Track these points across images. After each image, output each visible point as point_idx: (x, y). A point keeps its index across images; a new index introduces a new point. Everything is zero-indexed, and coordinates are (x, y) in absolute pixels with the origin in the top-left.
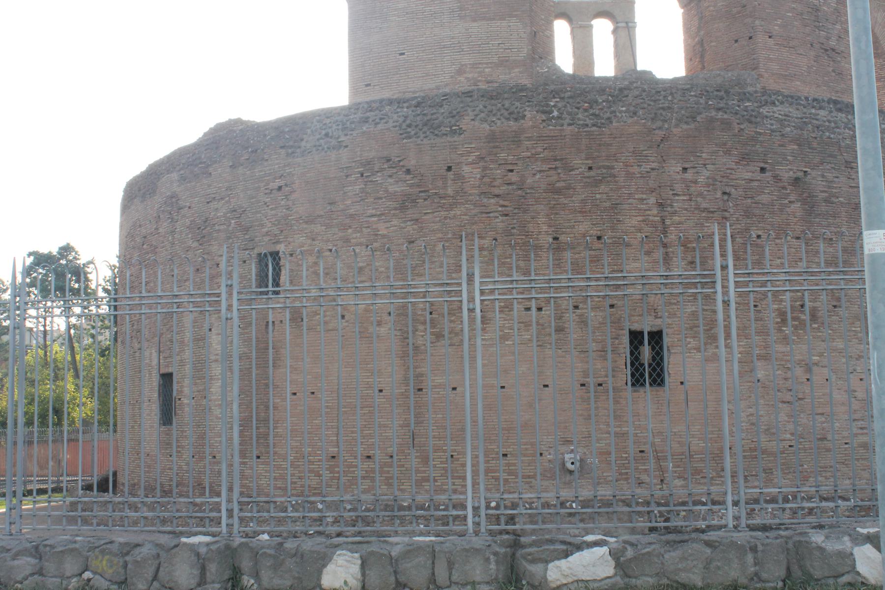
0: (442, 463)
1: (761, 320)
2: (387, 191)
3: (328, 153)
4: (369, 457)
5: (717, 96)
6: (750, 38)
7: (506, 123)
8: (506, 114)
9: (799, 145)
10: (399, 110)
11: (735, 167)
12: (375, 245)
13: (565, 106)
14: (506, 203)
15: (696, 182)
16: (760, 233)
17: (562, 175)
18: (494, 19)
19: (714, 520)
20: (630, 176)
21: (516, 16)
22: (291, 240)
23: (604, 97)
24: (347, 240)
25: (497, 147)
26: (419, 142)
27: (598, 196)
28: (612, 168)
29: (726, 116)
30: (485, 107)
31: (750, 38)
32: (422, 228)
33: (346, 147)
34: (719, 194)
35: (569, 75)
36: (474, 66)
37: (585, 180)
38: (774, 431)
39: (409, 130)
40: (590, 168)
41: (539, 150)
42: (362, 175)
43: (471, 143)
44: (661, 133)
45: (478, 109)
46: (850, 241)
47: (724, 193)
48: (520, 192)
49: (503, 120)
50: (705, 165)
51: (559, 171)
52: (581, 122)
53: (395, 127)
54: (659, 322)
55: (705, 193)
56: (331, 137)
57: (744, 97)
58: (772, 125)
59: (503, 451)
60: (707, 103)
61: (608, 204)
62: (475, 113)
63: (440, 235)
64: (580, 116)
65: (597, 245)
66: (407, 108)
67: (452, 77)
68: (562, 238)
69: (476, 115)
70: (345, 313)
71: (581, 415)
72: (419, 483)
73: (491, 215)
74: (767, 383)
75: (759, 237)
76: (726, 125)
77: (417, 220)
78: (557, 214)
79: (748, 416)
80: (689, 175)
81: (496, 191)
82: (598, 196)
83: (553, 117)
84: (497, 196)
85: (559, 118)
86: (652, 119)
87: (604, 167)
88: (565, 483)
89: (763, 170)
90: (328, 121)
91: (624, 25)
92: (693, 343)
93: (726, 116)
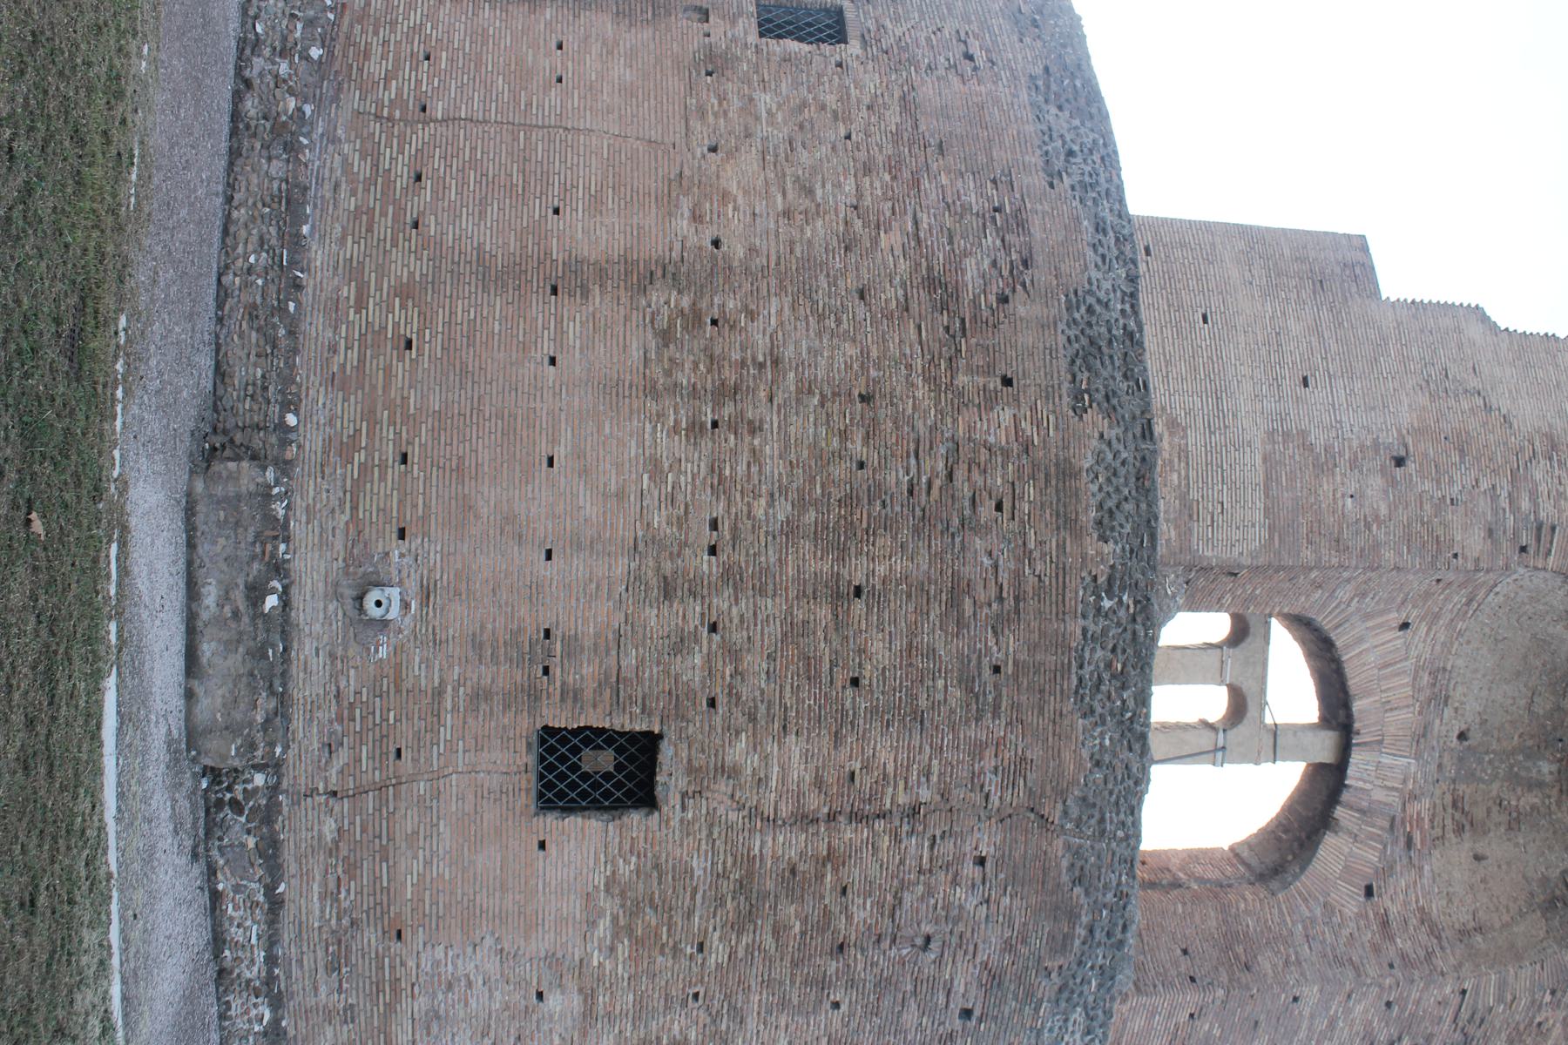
0: (396, 325)
1: (667, 1008)
2: (966, 254)
3: (1038, 152)
4: (419, 178)
5: (1116, 925)
6: (1193, 979)
7: (1093, 502)
8: (1111, 504)
10: (1119, 294)
11: (978, 960)
12: (858, 224)
13: (1119, 624)
14: (935, 492)
15: (955, 882)
16: (844, 1007)
17: (986, 610)
18: (1267, 496)
19: (236, 908)
20: (977, 750)
21: (1271, 538)
22: (870, 67)
23: (1131, 703)
24: (868, 169)
25: (1047, 481)
26: (1061, 326)
27: (940, 683)
28: (996, 714)
29: (1077, 942)
30: (1123, 463)
31: (1193, 979)
32: (889, 316)
33: (1052, 186)
34: (927, 928)
35: (1154, 639)
36: (1183, 453)
37: (974, 657)
38: (435, 1028)
39: (1083, 309)
40: (997, 670)
41: (1039, 568)
42: (996, 210)
43: (1056, 428)
44: (1056, 816)
45: (1121, 447)
47: (928, 939)
48: (956, 521)
49: (1099, 497)
50: (987, 901)
51: (995, 606)
52: (1087, 655)
53: (1090, 283)
54: (675, 800)
55: (932, 901)
56: (1067, 161)
57: (1107, 975)
58: (1051, 1030)
59: (415, 455)
60: (1105, 906)
61: (923, 703)
62: (1114, 442)
63: (874, 354)
64: (1099, 653)
65: (841, 677)
66: (1123, 311)
67: (1163, 409)
68: (859, 606)
69: (1109, 444)
70: (721, 154)
71: (482, 627)
72: (354, 272)
73: (913, 461)
74: (535, 1017)
75: (836, 1005)
76: (1060, 944)
77: (907, 310)
78: (909, 596)
79: (467, 976)
80: (970, 870)
81: (960, 473)
82: (940, 683)
83: (1100, 598)
84: (950, 476)
85: (1099, 609)
86: (1084, 799)
87: (998, 698)
88: (337, 585)
89: (967, 1013)
90: (1096, 157)
91: (1220, 743)
92: (626, 870)
93: (1077, 942)
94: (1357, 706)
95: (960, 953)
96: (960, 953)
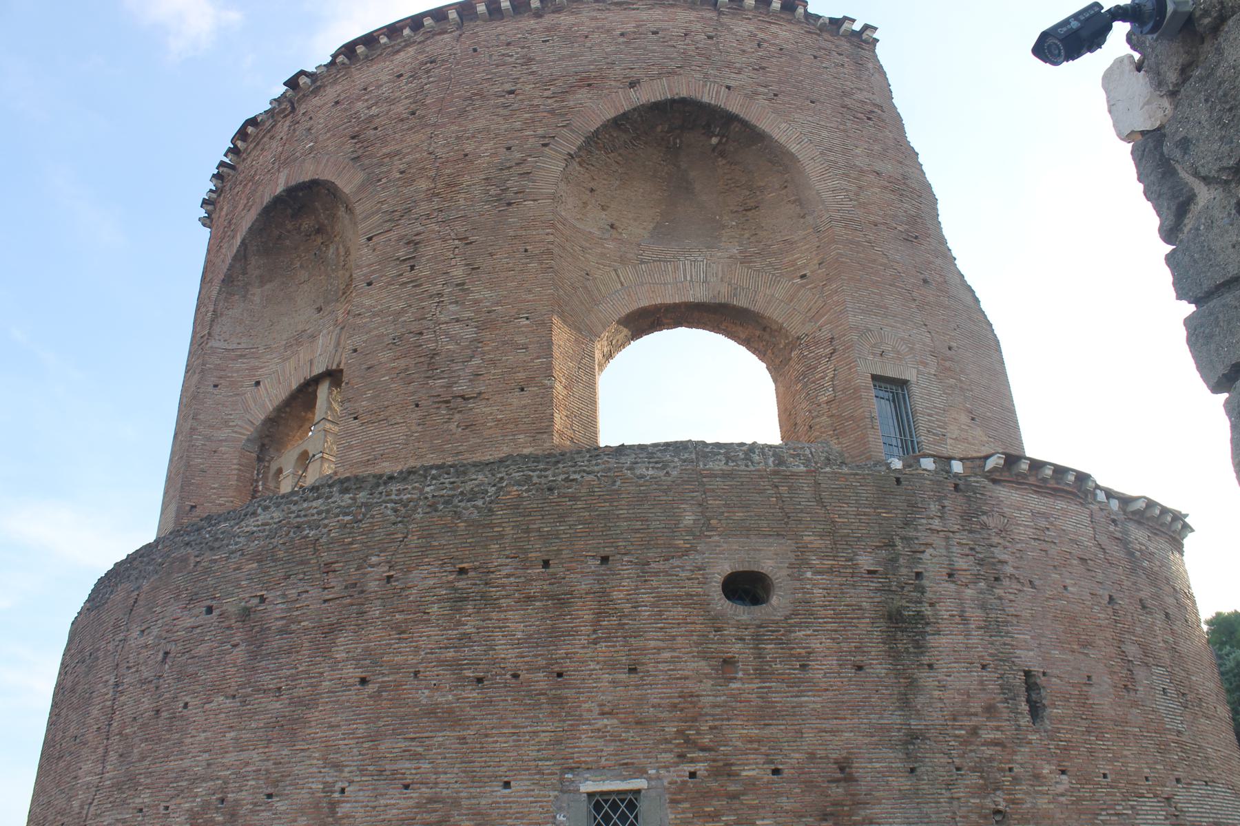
9: (259, 561)
16: (187, 699)
28: (98, 649)
34: (161, 655)
46: (311, 685)
75: (186, 706)
89: (210, 610)
94: (294, 386)
95: (175, 629)
96: (175, 629)
